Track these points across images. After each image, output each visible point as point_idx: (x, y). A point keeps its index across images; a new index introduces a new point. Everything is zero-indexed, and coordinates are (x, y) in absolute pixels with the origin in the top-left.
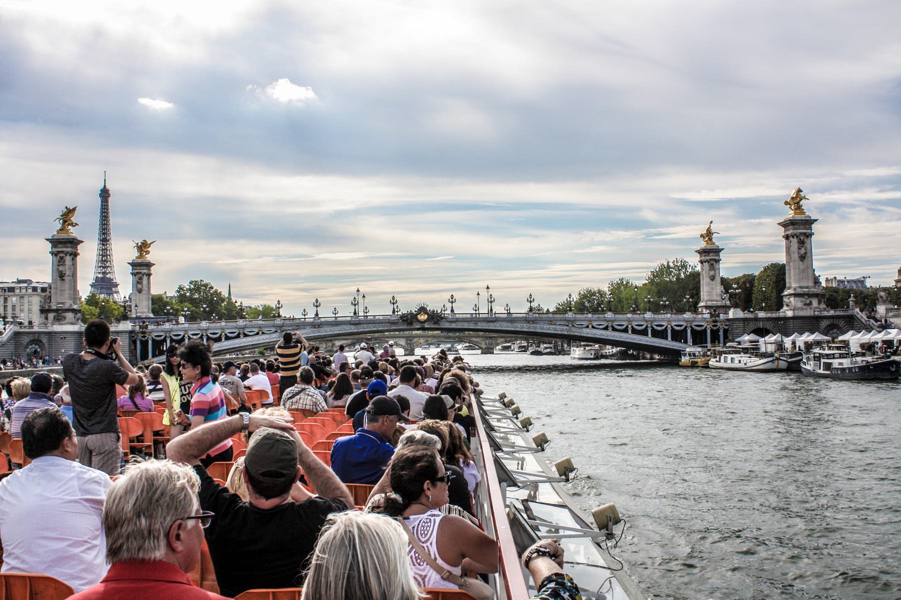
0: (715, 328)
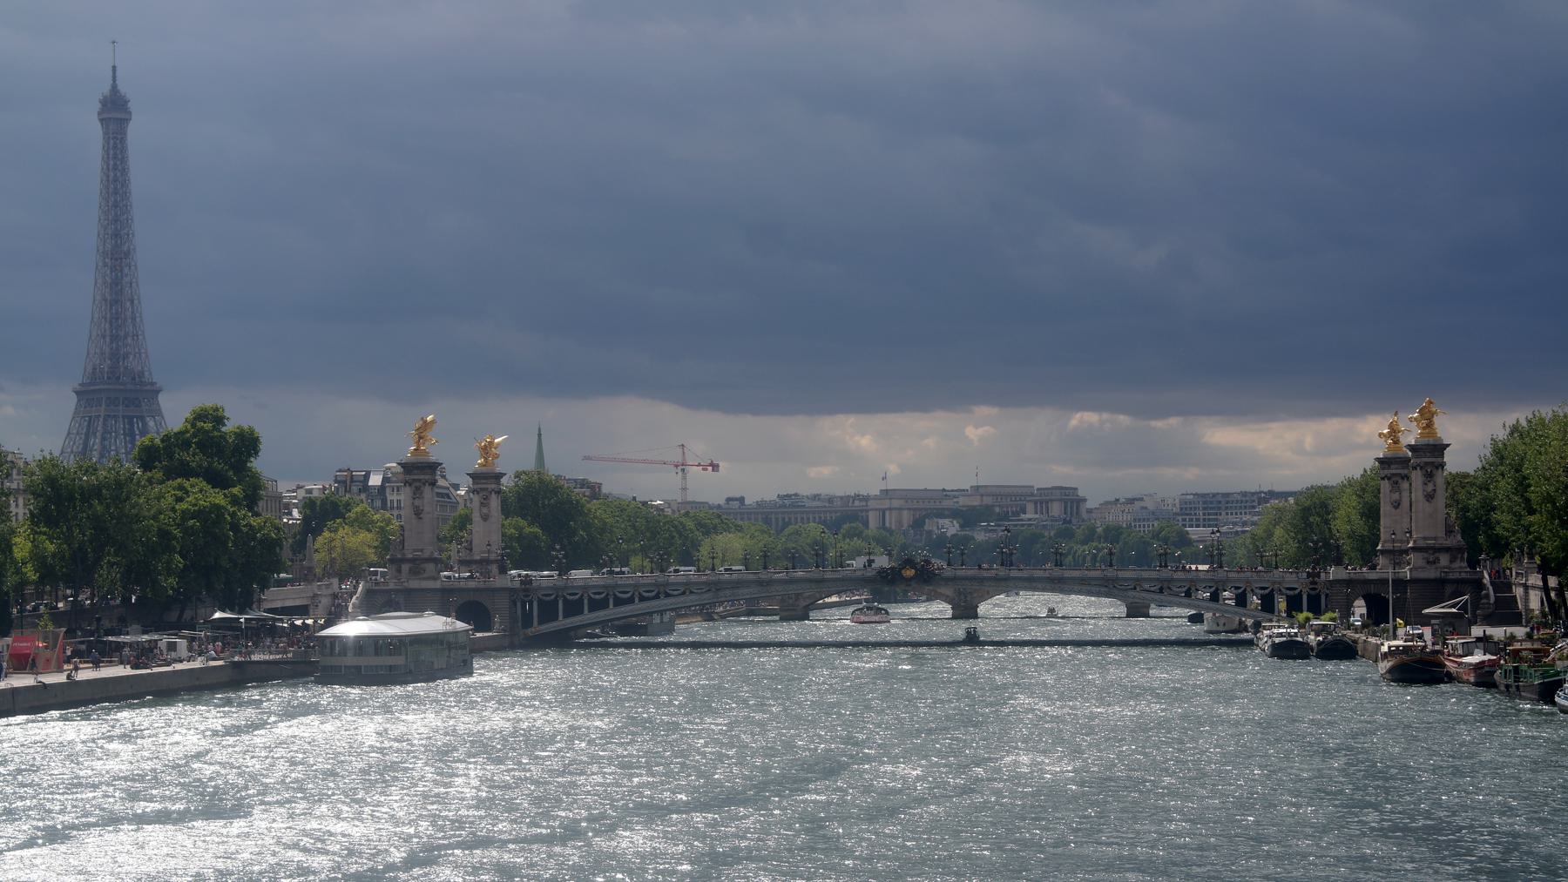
0: (1313, 593)
